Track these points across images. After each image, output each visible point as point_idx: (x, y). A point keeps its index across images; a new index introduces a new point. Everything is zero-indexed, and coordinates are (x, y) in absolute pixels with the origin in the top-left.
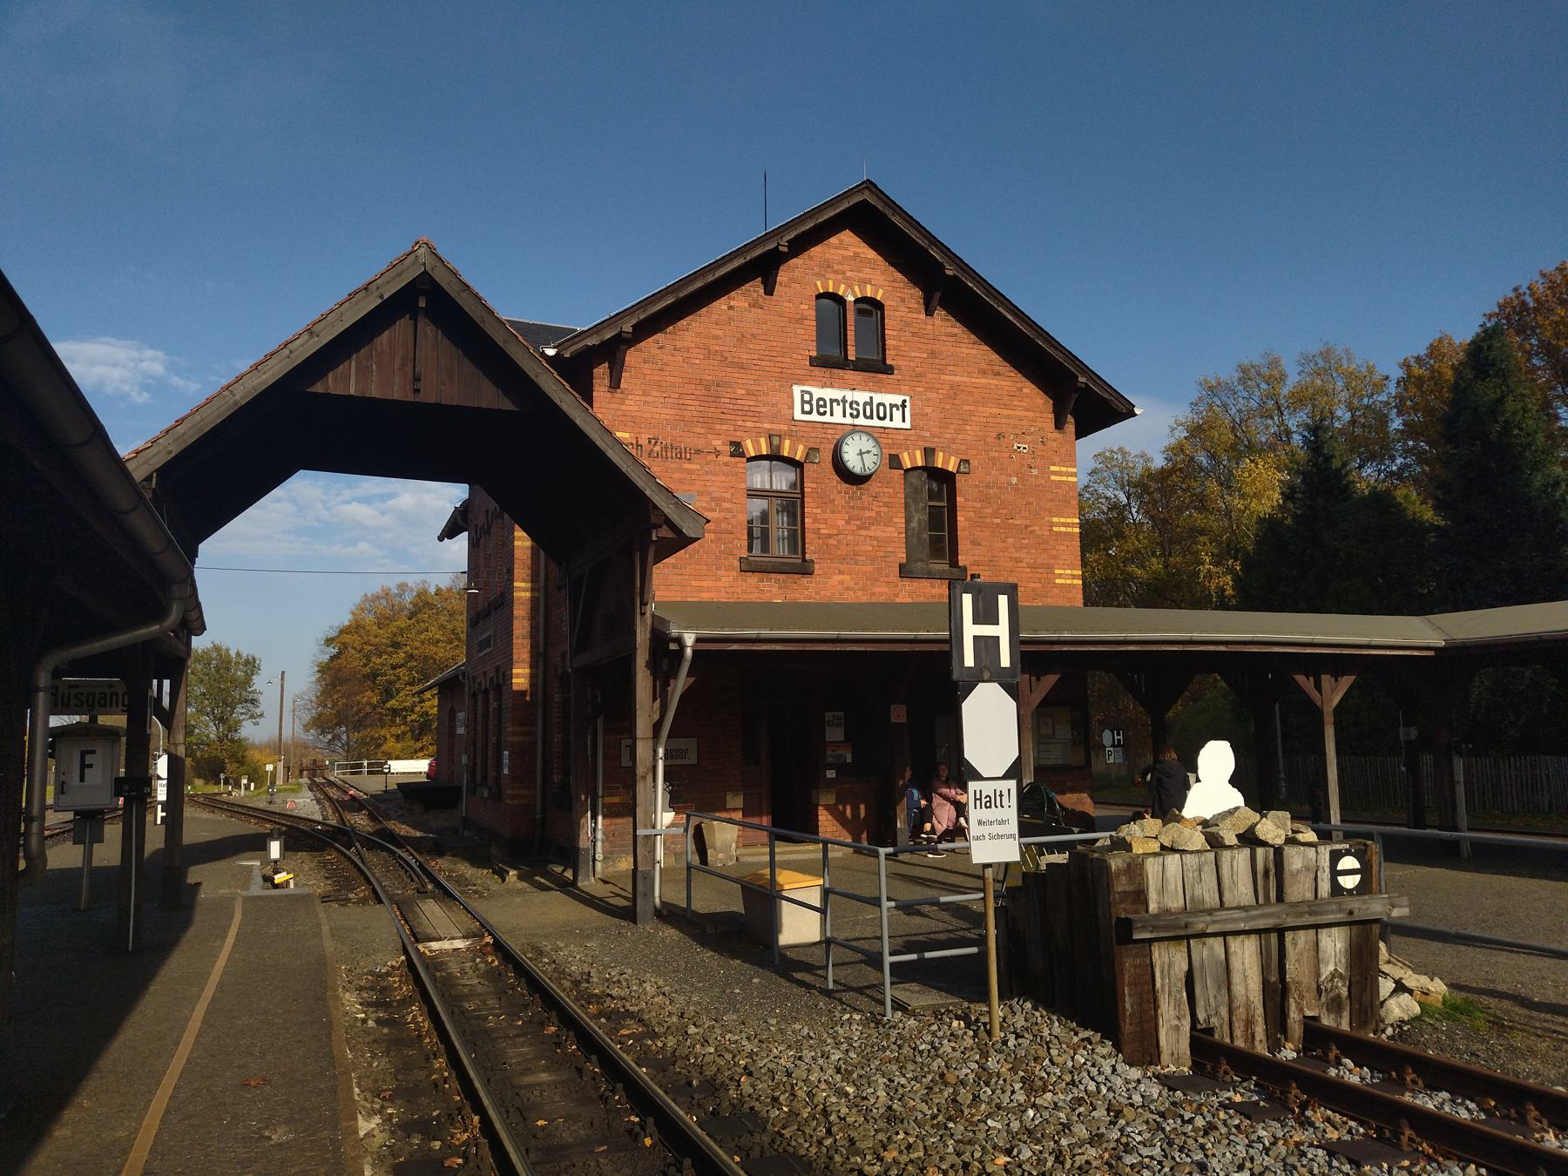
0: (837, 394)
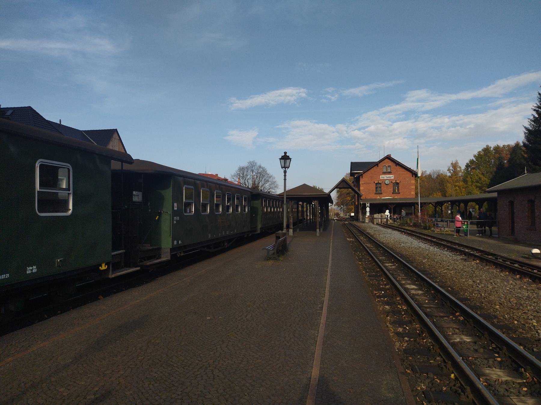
0: (385, 176)
